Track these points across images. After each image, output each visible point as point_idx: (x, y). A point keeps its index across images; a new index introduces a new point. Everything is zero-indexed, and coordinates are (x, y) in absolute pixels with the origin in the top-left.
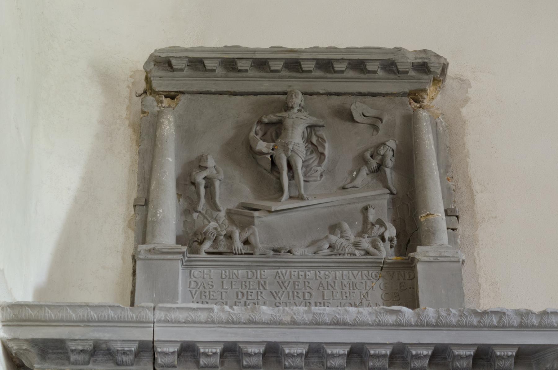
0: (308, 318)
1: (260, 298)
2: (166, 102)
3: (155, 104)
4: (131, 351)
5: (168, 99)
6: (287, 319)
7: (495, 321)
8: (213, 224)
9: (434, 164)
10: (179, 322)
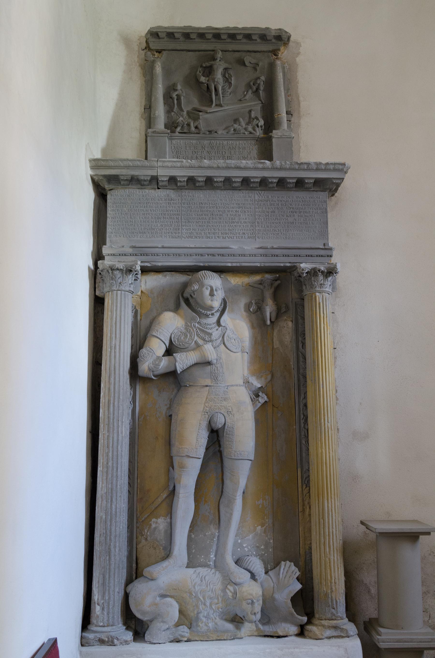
0: (224, 165)
1: (203, 154)
2: (157, 54)
3: (152, 56)
4: (147, 180)
5: (158, 53)
6: (215, 166)
7: (306, 167)
8: (181, 119)
9: (282, 89)
10: (168, 167)
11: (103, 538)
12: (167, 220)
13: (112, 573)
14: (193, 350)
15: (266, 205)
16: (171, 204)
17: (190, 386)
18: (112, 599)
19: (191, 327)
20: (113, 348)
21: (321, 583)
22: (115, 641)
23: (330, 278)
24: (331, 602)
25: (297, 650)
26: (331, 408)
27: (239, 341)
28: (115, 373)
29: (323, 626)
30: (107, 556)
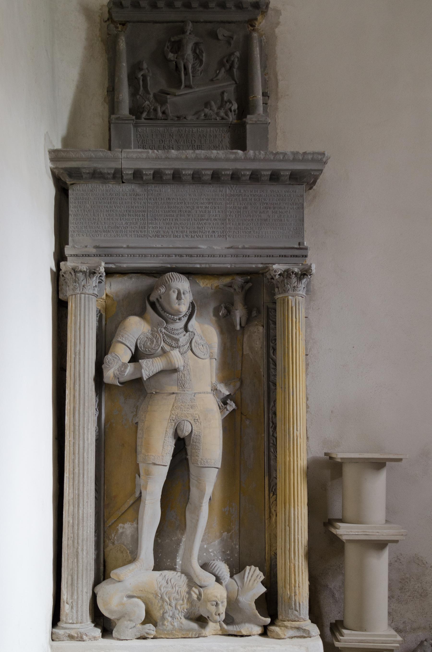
1: (171, 143)
2: (120, 27)
3: (115, 29)
5: (121, 26)
8: (147, 102)
9: (258, 66)
11: (71, 542)
12: (133, 217)
13: (80, 575)
14: (160, 356)
15: (238, 200)
16: (136, 200)
17: (156, 393)
18: (80, 598)
19: (157, 332)
20: (78, 353)
21: (285, 587)
22: (84, 637)
23: (304, 281)
24: (294, 604)
25: (259, 648)
26: (300, 416)
27: (208, 347)
28: (80, 380)
29: (286, 627)
30: (74, 558)
